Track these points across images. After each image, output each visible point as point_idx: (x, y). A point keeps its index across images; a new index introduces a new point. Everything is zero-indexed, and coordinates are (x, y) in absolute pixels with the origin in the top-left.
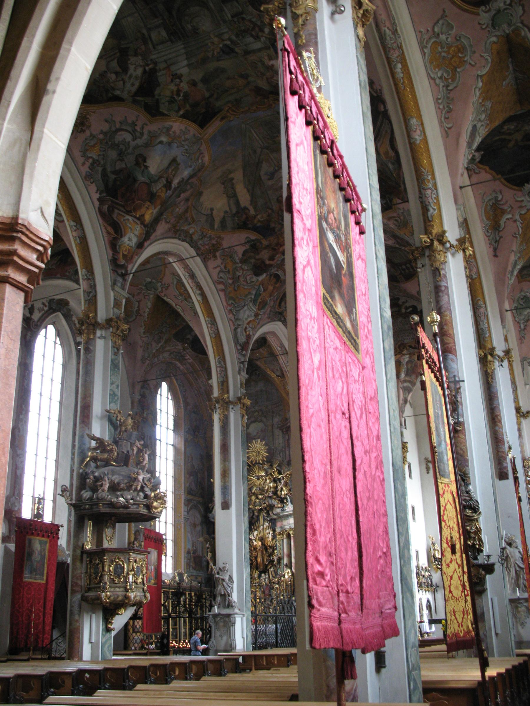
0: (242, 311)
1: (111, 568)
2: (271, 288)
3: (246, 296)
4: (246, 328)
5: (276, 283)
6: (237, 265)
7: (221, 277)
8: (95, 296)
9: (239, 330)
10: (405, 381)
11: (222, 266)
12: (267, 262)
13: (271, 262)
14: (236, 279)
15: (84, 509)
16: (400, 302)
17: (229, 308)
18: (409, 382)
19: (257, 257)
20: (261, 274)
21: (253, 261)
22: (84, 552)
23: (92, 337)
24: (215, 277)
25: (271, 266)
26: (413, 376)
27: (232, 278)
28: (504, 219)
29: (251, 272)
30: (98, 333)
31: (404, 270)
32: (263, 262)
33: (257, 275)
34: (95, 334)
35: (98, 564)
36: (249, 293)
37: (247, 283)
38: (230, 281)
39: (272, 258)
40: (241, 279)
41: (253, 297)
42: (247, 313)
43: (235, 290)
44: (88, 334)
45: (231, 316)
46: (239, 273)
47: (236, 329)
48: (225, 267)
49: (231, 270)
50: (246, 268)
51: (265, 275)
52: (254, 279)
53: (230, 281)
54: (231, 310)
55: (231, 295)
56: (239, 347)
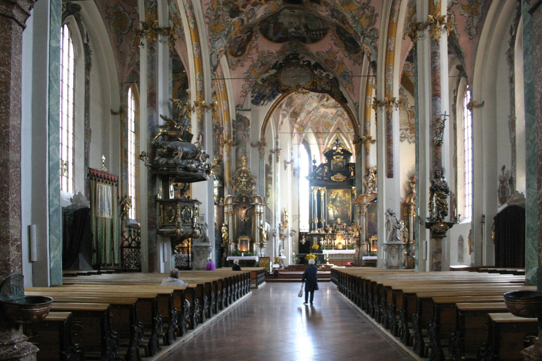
0: (217, 42)
2: (237, 29)
3: (222, 31)
4: (218, 55)
5: (241, 26)
6: (220, 6)
7: (208, 13)
8: (156, 6)
9: (213, 55)
10: (284, 110)
11: (211, 5)
12: (241, 9)
13: (243, 10)
14: (217, 17)
15: (163, 170)
16: (300, 57)
17: (209, 38)
18: (287, 111)
19: (235, 3)
20: (235, 17)
21: (231, 5)
23: (155, 39)
24: (205, 11)
25: (242, 12)
26: (289, 108)
27: (215, 16)
29: (228, 14)
30: (160, 37)
31: (313, 35)
32: (238, 8)
33: (232, 17)
34: (157, 37)
36: (224, 30)
37: (224, 21)
38: (213, 18)
39: (244, 6)
40: (221, 18)
41: (226, 33)
42: (220, 44)
43: (215, 26)
44: (152, 36)
45: (210, 44)
46: (220, 13)
47: (211, 54)
48: (212, 6)
49: (215, 9)
50: (225, 10)
51: (237, 18)
52: (230, 19)
53: (213, 18)
54: (210, 39)
55: (212, 28)
56: (212, 68)
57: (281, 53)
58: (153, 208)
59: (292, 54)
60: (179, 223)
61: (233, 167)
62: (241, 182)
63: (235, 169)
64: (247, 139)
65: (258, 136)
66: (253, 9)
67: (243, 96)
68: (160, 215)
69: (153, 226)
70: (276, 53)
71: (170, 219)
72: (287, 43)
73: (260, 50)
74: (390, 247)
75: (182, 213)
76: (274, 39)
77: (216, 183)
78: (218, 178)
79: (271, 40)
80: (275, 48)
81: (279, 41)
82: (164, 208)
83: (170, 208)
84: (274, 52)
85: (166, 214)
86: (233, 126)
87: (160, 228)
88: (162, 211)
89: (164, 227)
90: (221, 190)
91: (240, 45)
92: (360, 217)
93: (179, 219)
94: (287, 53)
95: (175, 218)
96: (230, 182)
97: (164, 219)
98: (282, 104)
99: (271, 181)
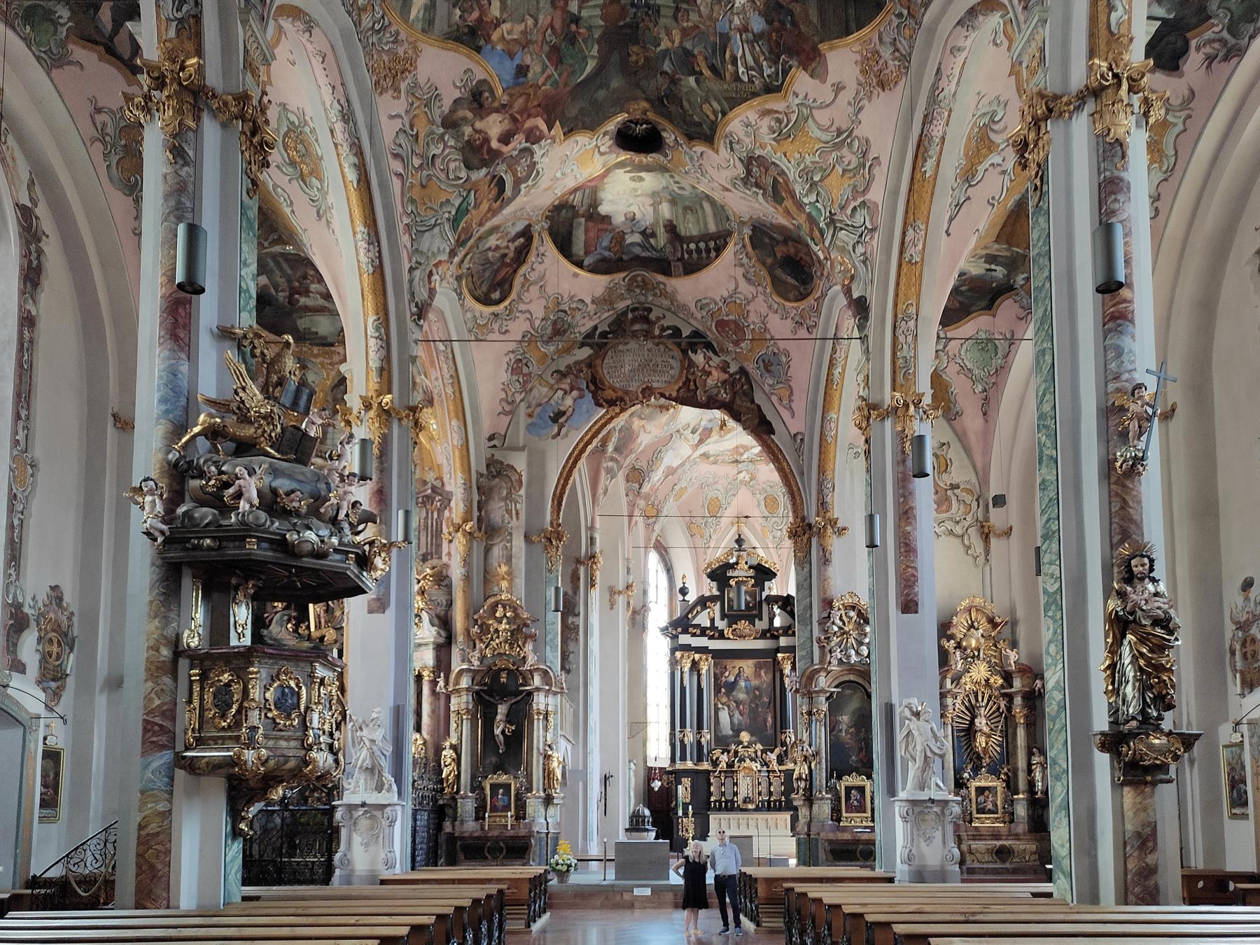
1: (268, 695)
22: (178, 652)
28: (986, 164)
35: (228, 685)
57: (604, 301)
58: (167, 680)
59: (633, 310)
60: (254, 729)
61: (477, 590)
62: (497, 631)
63: (482, 598)
64: (514, 522)
65: (544, 518)
66: (532, 154)
67: (504, 413)
68: (190, 702)
69: (163, 739)
70: (593, 302)
71: (223, 717)
72: (619, 276)
73: (550, 290)
74: (917, 809)
75: (268, 695)
76: (586, 263)
77: (427, 632)
78: (436, 621)
79: (579, 264)
80: (589, 286)
81: (603, 267)
82: (204, 677)
83: (226, 677)
84: (588, 301)
85: (208, 697)
86: (478, 489)
87: (187, 749)
88: (196, 688)
89: (201, 742)
90: (443, 649)
91: (498, 271)
92: (810, 726)
93: (254, 717)
94: (621, 305)
95: (239, 711)
96: (467, 631)
97: (201, 716)
98: (604, 442)
99: (577, 633)
